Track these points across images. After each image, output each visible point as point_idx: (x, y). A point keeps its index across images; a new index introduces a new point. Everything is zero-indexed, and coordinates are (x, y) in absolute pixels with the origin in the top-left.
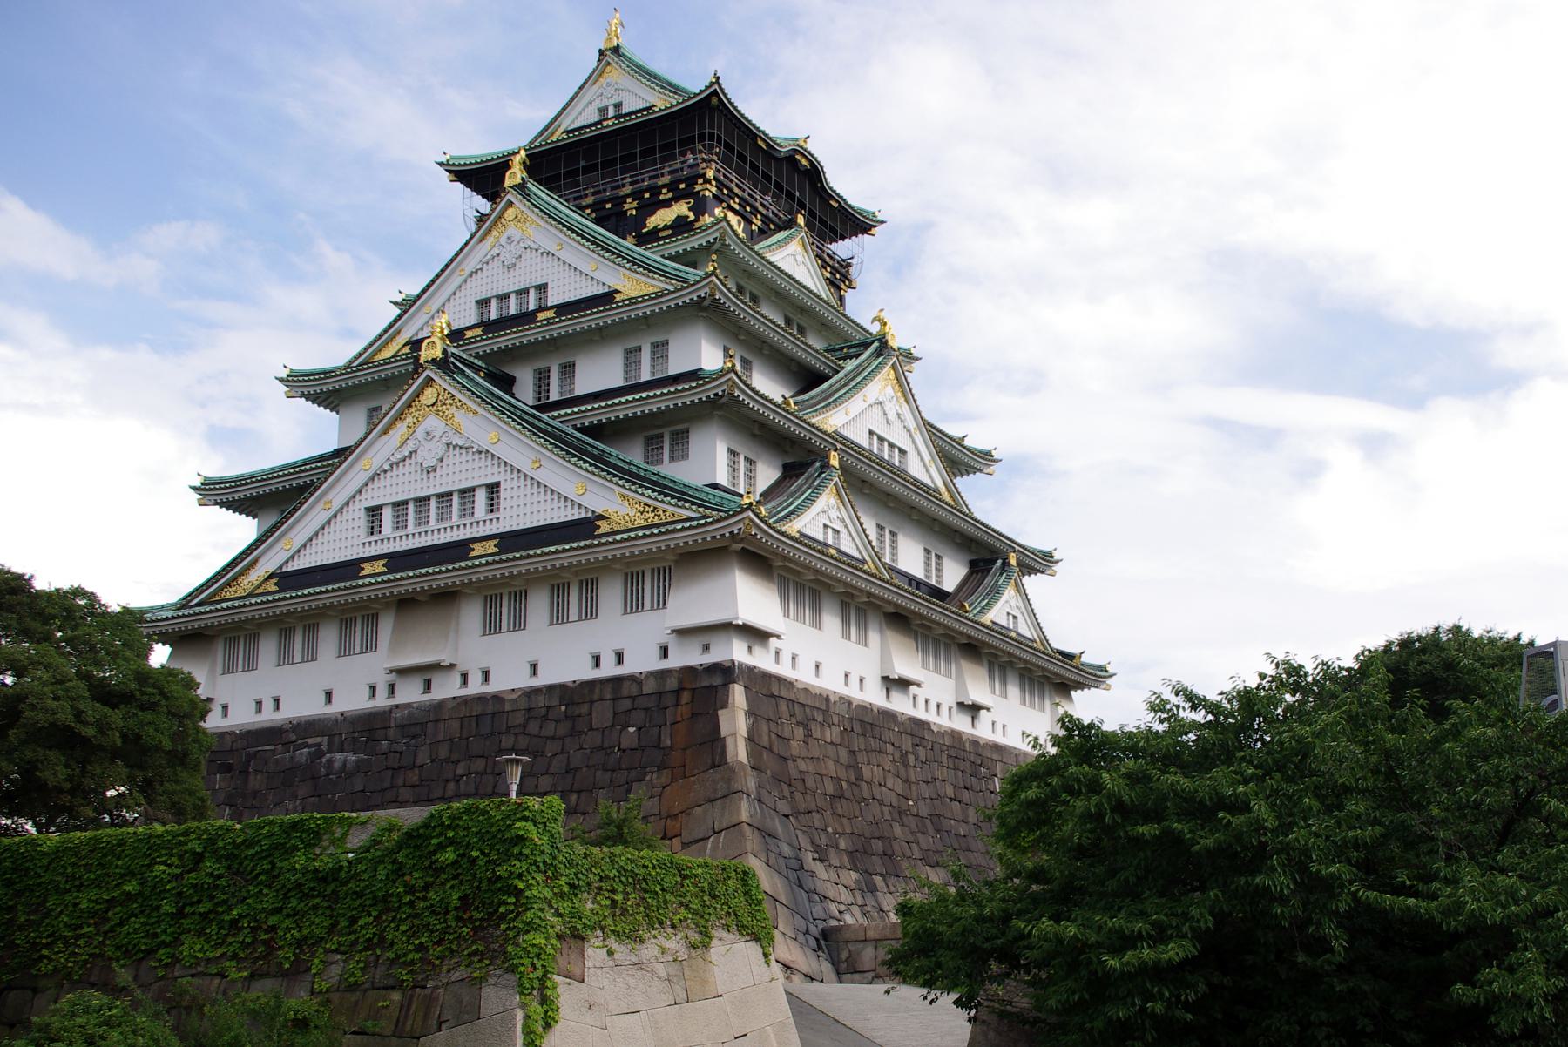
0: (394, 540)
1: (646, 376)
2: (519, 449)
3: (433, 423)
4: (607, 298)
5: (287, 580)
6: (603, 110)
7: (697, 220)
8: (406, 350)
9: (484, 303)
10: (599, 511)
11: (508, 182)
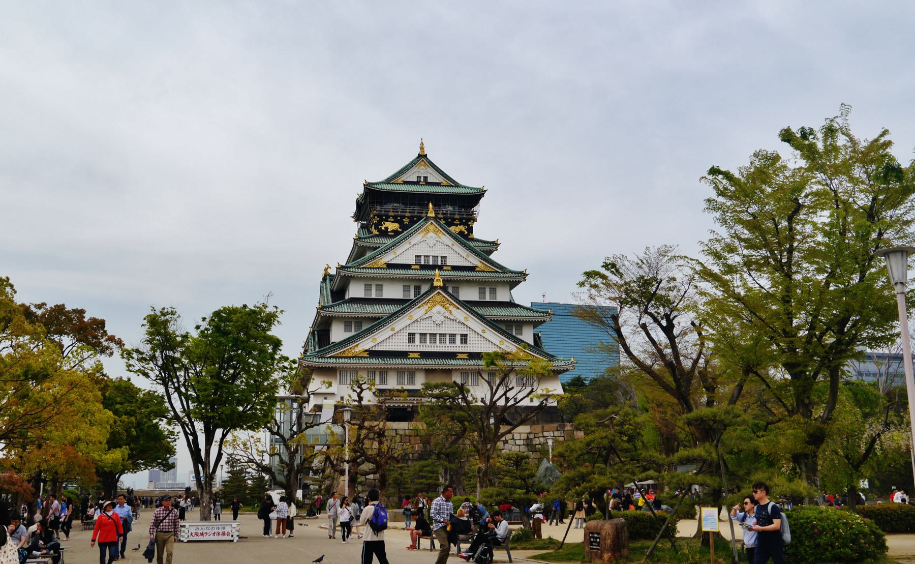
0: (418, 346)
1: (488, 299)
2: (475, 324)
3: (438, 308)
4: (472, 269)
5: (373, 354)
6: (419, 177)
7: (468, 234)
8: (385, 266)
9: (418, 257)
10: (509, 350)
11: (429, 215)
